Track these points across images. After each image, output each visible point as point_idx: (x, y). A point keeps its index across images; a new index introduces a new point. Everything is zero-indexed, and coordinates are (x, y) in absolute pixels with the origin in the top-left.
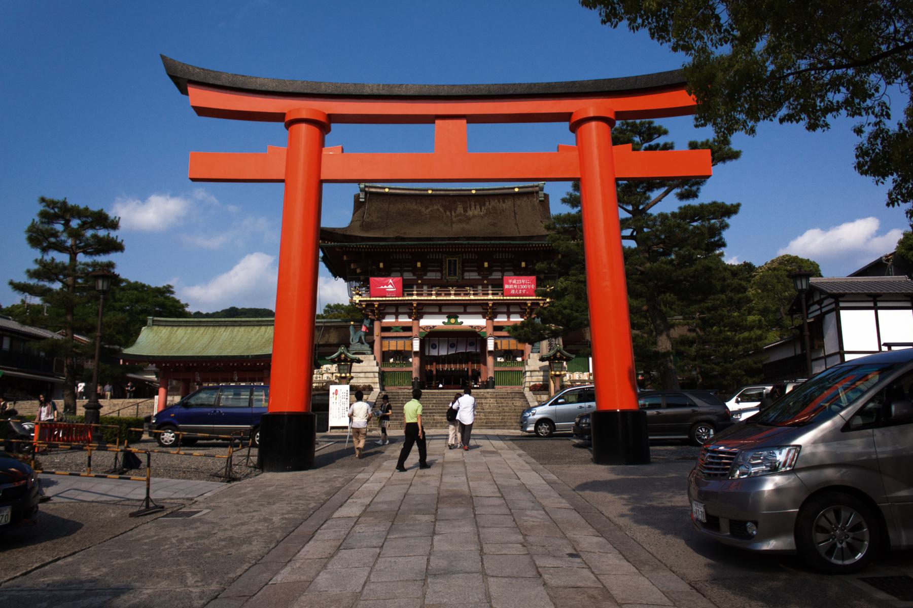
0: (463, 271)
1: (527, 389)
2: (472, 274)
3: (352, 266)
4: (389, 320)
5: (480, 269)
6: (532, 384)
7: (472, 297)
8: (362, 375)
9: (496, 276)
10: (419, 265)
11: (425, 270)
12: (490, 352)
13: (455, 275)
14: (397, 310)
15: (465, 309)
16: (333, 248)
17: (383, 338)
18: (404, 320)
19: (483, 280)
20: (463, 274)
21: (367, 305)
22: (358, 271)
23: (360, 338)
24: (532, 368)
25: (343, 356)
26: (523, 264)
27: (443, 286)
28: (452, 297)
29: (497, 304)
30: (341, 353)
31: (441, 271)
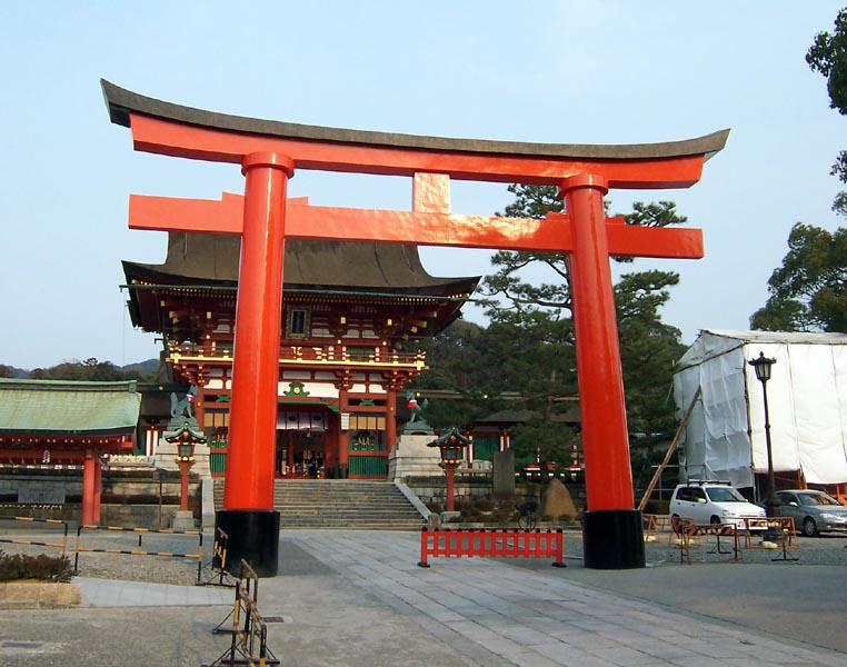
0: (312, 327)
2: (319, 331)
3: (171, 314)
5: (333, 325)
7: (324, 362)
9: (353, 334)
12: (345, 431)
13: (301, 332)
15: (313, 377)
16: (149, 290)
19: (335, 339)
22: (175, 321)
23: (186, 409)
25: (186, 434)
26: (390, 322)
28: (300, 361)
29: (355, 370)
30: (184, 430)
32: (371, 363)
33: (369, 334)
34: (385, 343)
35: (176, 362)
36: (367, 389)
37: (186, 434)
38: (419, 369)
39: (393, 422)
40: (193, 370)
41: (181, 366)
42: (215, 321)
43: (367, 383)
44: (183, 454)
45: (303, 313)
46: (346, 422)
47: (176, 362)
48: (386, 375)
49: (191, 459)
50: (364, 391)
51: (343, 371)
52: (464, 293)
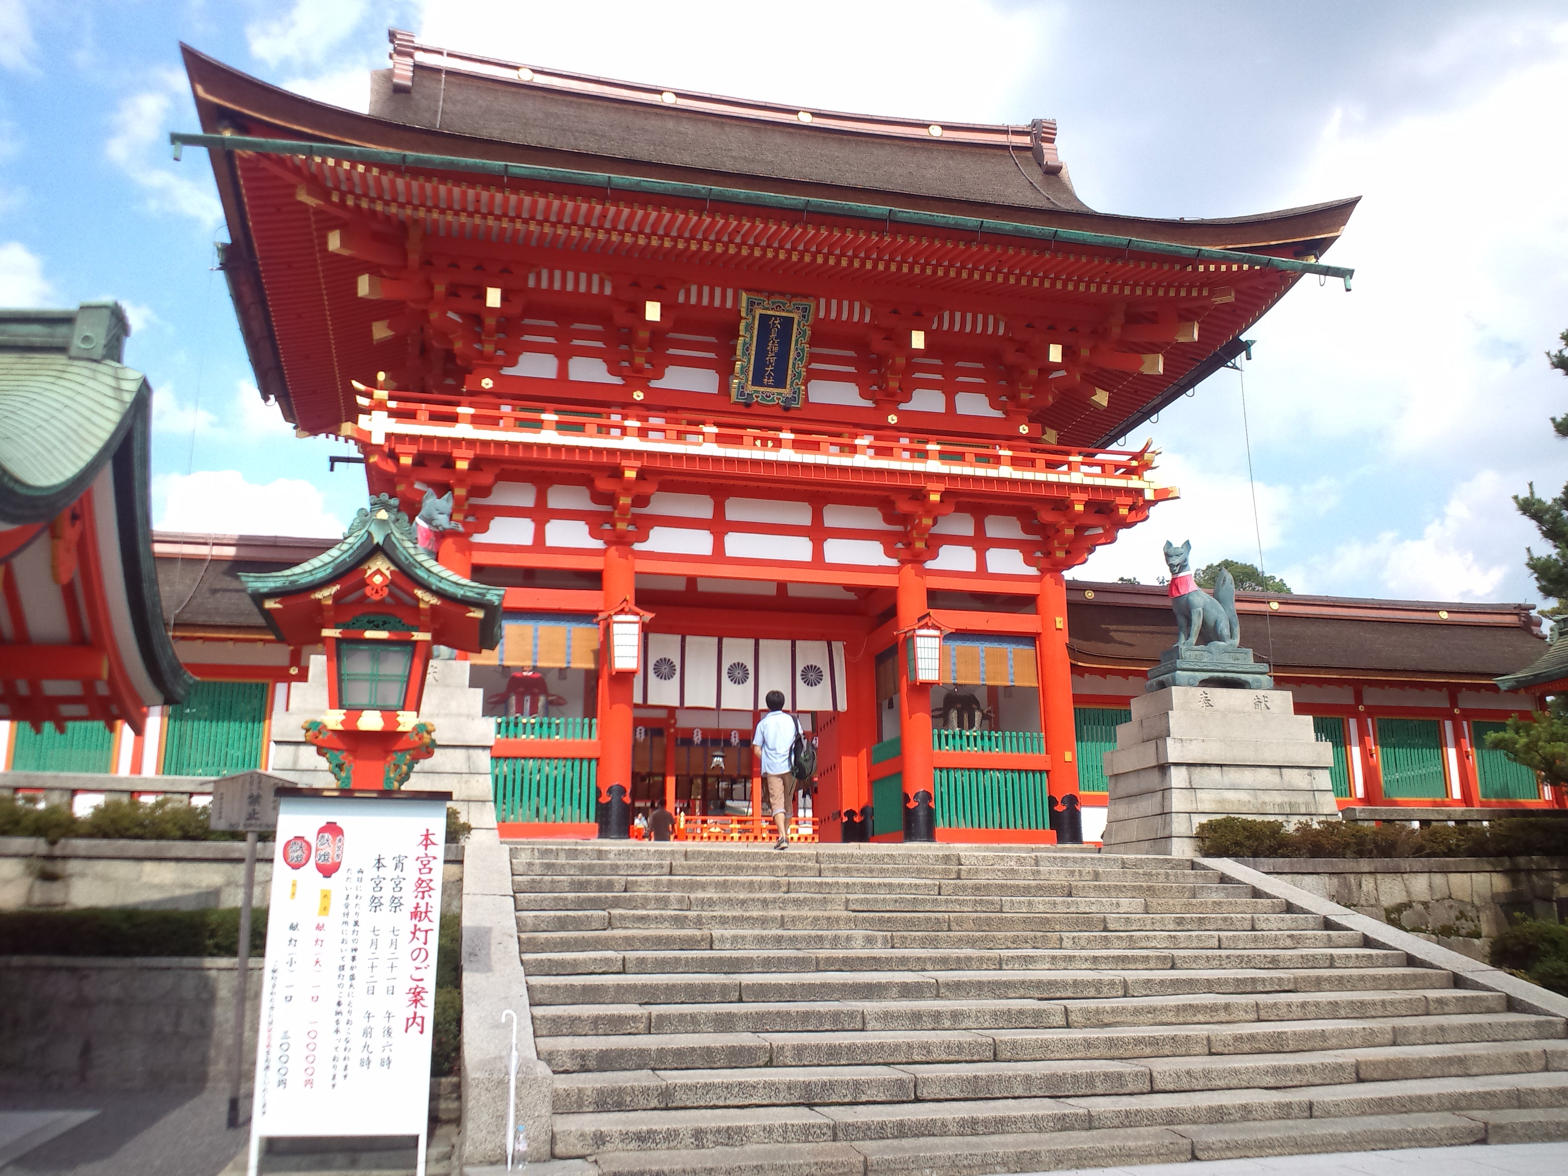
1: (1182, 849)
3: (364, 286)
10: (653, 311)
13: (780, 382)
14: (541, 498)
21: (420, 460)
25: (379, 571)
26: (1055, 354)
33: (973, 405)
34: (1024, 429)
37: (379, 571)
38: (1149, 495)
39: (1061, 662)
41: (394, 456)
43: (981, 543)
44: (358, 694)
45: (788, 322)
46: (929, 658)
47: (378, 439)
48: (1047, 516)
50: (972, 567)
51: (919, 495)
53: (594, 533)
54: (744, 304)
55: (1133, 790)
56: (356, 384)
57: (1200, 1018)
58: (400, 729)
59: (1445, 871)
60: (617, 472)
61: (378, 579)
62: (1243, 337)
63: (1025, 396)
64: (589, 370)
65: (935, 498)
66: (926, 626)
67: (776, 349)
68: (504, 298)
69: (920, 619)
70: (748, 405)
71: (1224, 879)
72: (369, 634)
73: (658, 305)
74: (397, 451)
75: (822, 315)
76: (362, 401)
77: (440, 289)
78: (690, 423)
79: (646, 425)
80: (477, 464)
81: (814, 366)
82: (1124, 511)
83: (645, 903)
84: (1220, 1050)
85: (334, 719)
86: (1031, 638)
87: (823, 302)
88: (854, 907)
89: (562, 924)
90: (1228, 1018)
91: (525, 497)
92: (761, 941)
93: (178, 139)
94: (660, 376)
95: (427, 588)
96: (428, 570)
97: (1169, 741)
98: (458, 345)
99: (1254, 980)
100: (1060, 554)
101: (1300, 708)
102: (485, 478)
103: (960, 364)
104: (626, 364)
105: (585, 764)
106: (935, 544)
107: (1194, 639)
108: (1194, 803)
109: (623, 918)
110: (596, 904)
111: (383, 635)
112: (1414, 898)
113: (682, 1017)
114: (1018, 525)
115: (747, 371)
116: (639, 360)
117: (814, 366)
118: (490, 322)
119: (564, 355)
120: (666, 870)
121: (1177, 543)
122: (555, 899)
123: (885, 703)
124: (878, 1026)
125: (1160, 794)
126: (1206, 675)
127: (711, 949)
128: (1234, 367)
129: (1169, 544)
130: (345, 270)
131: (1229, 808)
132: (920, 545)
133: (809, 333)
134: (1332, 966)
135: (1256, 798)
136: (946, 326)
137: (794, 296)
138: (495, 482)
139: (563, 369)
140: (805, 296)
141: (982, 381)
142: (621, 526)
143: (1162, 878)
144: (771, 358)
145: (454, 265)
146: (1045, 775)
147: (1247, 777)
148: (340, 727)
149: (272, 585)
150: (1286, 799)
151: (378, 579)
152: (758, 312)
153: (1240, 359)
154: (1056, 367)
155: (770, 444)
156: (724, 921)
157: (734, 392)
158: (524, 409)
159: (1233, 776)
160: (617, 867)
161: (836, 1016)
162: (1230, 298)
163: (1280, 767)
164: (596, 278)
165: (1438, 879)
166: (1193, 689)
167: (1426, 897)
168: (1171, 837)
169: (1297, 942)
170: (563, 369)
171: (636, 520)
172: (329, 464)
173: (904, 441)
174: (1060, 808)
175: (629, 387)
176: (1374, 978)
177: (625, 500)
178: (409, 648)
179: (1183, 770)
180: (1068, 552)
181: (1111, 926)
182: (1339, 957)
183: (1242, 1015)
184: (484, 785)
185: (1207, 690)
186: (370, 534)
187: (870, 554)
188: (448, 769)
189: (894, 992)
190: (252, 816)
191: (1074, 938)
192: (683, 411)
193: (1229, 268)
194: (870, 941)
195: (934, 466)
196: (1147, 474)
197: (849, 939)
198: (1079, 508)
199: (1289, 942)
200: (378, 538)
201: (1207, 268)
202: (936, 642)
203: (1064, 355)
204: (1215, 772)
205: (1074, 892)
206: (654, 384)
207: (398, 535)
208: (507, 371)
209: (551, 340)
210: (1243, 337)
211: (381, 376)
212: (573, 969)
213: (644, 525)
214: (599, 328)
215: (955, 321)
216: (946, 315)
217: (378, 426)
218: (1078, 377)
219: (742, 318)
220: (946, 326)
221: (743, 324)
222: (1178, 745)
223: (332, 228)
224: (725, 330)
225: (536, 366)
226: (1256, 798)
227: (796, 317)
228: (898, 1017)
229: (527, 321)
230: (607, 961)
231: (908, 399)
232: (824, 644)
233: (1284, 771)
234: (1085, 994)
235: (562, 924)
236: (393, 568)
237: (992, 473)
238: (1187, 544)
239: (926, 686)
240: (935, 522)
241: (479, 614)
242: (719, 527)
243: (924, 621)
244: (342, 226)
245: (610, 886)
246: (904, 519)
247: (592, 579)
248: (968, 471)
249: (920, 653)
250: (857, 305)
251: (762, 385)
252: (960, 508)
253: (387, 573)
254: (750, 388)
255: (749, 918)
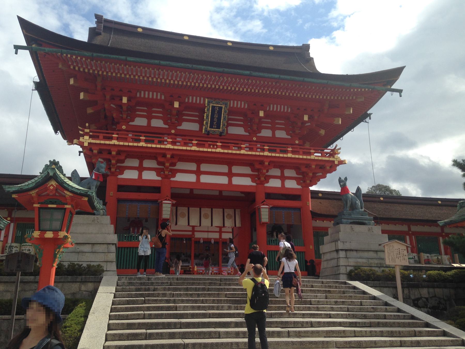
0: (229, 125)
1: (343, 278)
4: (130, 175)
6: (349, 269)
8: (87, 248)
10: (176, 105)
11: (179, 117)
13: (218, 127)
14: (141, 164)
17: (119, 200)
18: (150, 176)
20: (227, 127)
21: (100, 152)
24: (347, 246)
26: (306, 118)
27: (204, 138)
31: (201, 122)
32: (290, 155)
35: (86, 144)
36: (283, 184)
38: (336, 163)
40: (108, 157)
41: (91, 150)
42: (132, 112)
43: (283, 178)
44: (46, 225)
46: (265, 214)
48: (303, 169)
49: (62, 234)
51: (262, 163)
52: (385, 85)
53: (158, 175)
54: (206, 102)
55: (329, 258)
56: (79, 127)
57: (335, 335)
58: (59, 237)
59: (433, 287)
60: (164, 156)
61: (52, 188)
62: (369, 112)
63: (297, 132)
64: (157, 123)
65: (267, 163)
66: (264, 205)
67: (217, 117)
68: (128, 100)
69: (262, 202)
70: (208, 134)
71: (355, 288)
72: (50, 206)
73: (178, 103)
74: (93, 148)
75: (232, 105)
76: (81, 132)
77: (108, 97)
78: (190, 140)
79: (175, 141)
80: (119, 153)
81: (230, 122)
82: (328, 168)
83: (158, 295)
84: (339, 346)
85: (36, 234)
86: (299, 209)
87: (232, 102)
88: (228, 296)
89: (128, 302)
90: (344, 336)
91: (135, 163)
92: (193, 308)
93: (17, 48)
94: (180, 125)
95: (68, 190)
96: (68, 184)
97: (339, 242)
98: (114, 115)
99: (356, 323)
100: (308, 182)
101: (383, 232)
102: (122, 157)
103: (277, 121)
104: (169, 121)
105: (126, 249)
106: (267, 178)
107: (348, 209)
108: (346, 263)
109: (149, 300)
110: (141, 295)
111: (54, 206)
112: (423, 296)
113: (157, 334)
114: (295, 172)
115: (208, 124)
116: (173, 120)
117: (230, 122)
118: (124, 108)
119: (149, 118)
120: (169, 284)
121: (343, 178)
122: (128, 294)
123: (254, 229)
124: (224, 336)
125: (336, 260)
126: (352, 221)
127: (176, 310)
128: (366, 122)
129: (340, 178)
130: (77, 90)
131: (359, 264)
132: (263, 179)
133: (227, 112)
134: (385, 319)
135: (368, 261)
136: (271, 109)
137: (223, 100)
138: (125, 159)
139: (149, 123)
140: (226, 100)
141: (284, 126)
142: (166, 173)
143: (334, 287)
144: (216, 120)
145: (113, 90)
146: (304, 253)
147: (366, 254)
148: (38, 237)
149: (14, 189)
150: (379, 262)
151: (52, 188)
152: (211, 105)
153: (367, 119)
154: (306, 122)
155: (215, 147)
156: (183, 301)
157: (203, 130)
158: (136, 136)
159: (361, 254)
160: (153, 283)
161: (210, 333)
162: (363, 99)
163: (377, 251)
164: (159, 94)
165: (431, 290)
166: (347, 225)
167: (427, 296)
168: (340, 274)
169: (375, 310)
170: (149, 123)
171: (171, 170)
172: (79, 153)
173: (259, 146)
174: (308, 264)
175: (170, 129)
176: (399, 323)
177: (167, 164)
178: (63, 211)
179: (344, 252)
180: (310, 181)
181: (313, 303)
182: (388, 315)
183: (349, 335)
184: (113, 257)
185: (352, 225)
186: (48, 173)
187: (247, 182)
188: (101, 251)
189: (233, 325)
190: (18, 267)
191: (298, 307)
192: (187, 137)
193: (361, 90)
194: (229, 308)
195: (266, 153)
196: (336, 156)
197: (222, 307)
198: (314, 167)
199: (372, 310)
200: (51, 174)
201: (354, 90)
202: (267, 210)
203: (309, 118)
204: (355, 253)
205: (303, 292)
206: (178, 128)
207: (58, 173)
208: (131, 123)
209: (145, 114)
210: (369, 112)
211: (87, 125)
212: (127, 317)
213: (174, 173)
214: (161, 110)
215: (274, 108)
216: (272, 106)
217: (86, 140)
218: (314, 125)
219: (206, 107)
220: (271, 109)
221: (206, 110)
222: (342, 243)
223: (71, 77)
224: (201, 110)
225: (140, 122)
226: (368, 261)
227: (223, 106)
228: (231, 334)
229: (138, 108)
230: (139, 314)
231: (260, 132)
232: (233, 210)
233: (378, 253)
234: (298, 326)
235: (128, 302)
236: (57, 184)
237: (285, 156)
238: (346, 179)
239: (264, 223)
240: (267, 171)
241: (86, 199)
242: (198, 173)
243: (263, 203)
244: (75, 77)
245: (149, 290)
246: (258, 170)
247: (156, 189)
248: (277, 155)
249: (262, 213)
250: (243, 103)
251: (213, 128)
252: (275, 167)
253: (55, 186)
254: (209, 129)
255: (192, 300)
